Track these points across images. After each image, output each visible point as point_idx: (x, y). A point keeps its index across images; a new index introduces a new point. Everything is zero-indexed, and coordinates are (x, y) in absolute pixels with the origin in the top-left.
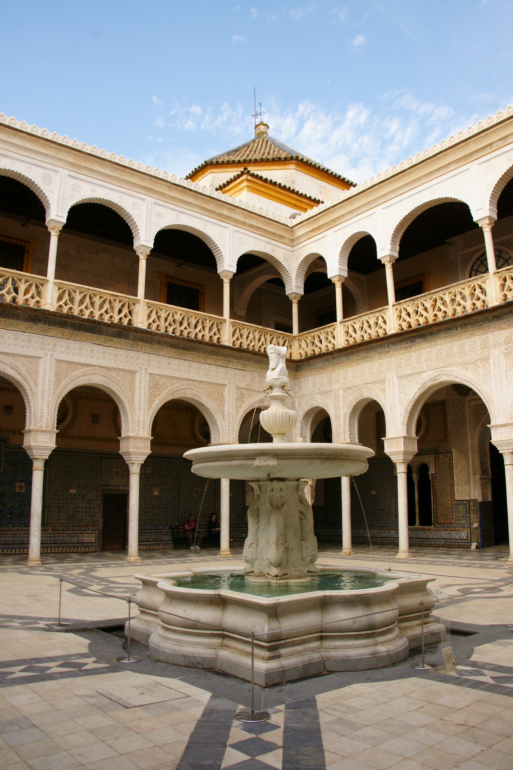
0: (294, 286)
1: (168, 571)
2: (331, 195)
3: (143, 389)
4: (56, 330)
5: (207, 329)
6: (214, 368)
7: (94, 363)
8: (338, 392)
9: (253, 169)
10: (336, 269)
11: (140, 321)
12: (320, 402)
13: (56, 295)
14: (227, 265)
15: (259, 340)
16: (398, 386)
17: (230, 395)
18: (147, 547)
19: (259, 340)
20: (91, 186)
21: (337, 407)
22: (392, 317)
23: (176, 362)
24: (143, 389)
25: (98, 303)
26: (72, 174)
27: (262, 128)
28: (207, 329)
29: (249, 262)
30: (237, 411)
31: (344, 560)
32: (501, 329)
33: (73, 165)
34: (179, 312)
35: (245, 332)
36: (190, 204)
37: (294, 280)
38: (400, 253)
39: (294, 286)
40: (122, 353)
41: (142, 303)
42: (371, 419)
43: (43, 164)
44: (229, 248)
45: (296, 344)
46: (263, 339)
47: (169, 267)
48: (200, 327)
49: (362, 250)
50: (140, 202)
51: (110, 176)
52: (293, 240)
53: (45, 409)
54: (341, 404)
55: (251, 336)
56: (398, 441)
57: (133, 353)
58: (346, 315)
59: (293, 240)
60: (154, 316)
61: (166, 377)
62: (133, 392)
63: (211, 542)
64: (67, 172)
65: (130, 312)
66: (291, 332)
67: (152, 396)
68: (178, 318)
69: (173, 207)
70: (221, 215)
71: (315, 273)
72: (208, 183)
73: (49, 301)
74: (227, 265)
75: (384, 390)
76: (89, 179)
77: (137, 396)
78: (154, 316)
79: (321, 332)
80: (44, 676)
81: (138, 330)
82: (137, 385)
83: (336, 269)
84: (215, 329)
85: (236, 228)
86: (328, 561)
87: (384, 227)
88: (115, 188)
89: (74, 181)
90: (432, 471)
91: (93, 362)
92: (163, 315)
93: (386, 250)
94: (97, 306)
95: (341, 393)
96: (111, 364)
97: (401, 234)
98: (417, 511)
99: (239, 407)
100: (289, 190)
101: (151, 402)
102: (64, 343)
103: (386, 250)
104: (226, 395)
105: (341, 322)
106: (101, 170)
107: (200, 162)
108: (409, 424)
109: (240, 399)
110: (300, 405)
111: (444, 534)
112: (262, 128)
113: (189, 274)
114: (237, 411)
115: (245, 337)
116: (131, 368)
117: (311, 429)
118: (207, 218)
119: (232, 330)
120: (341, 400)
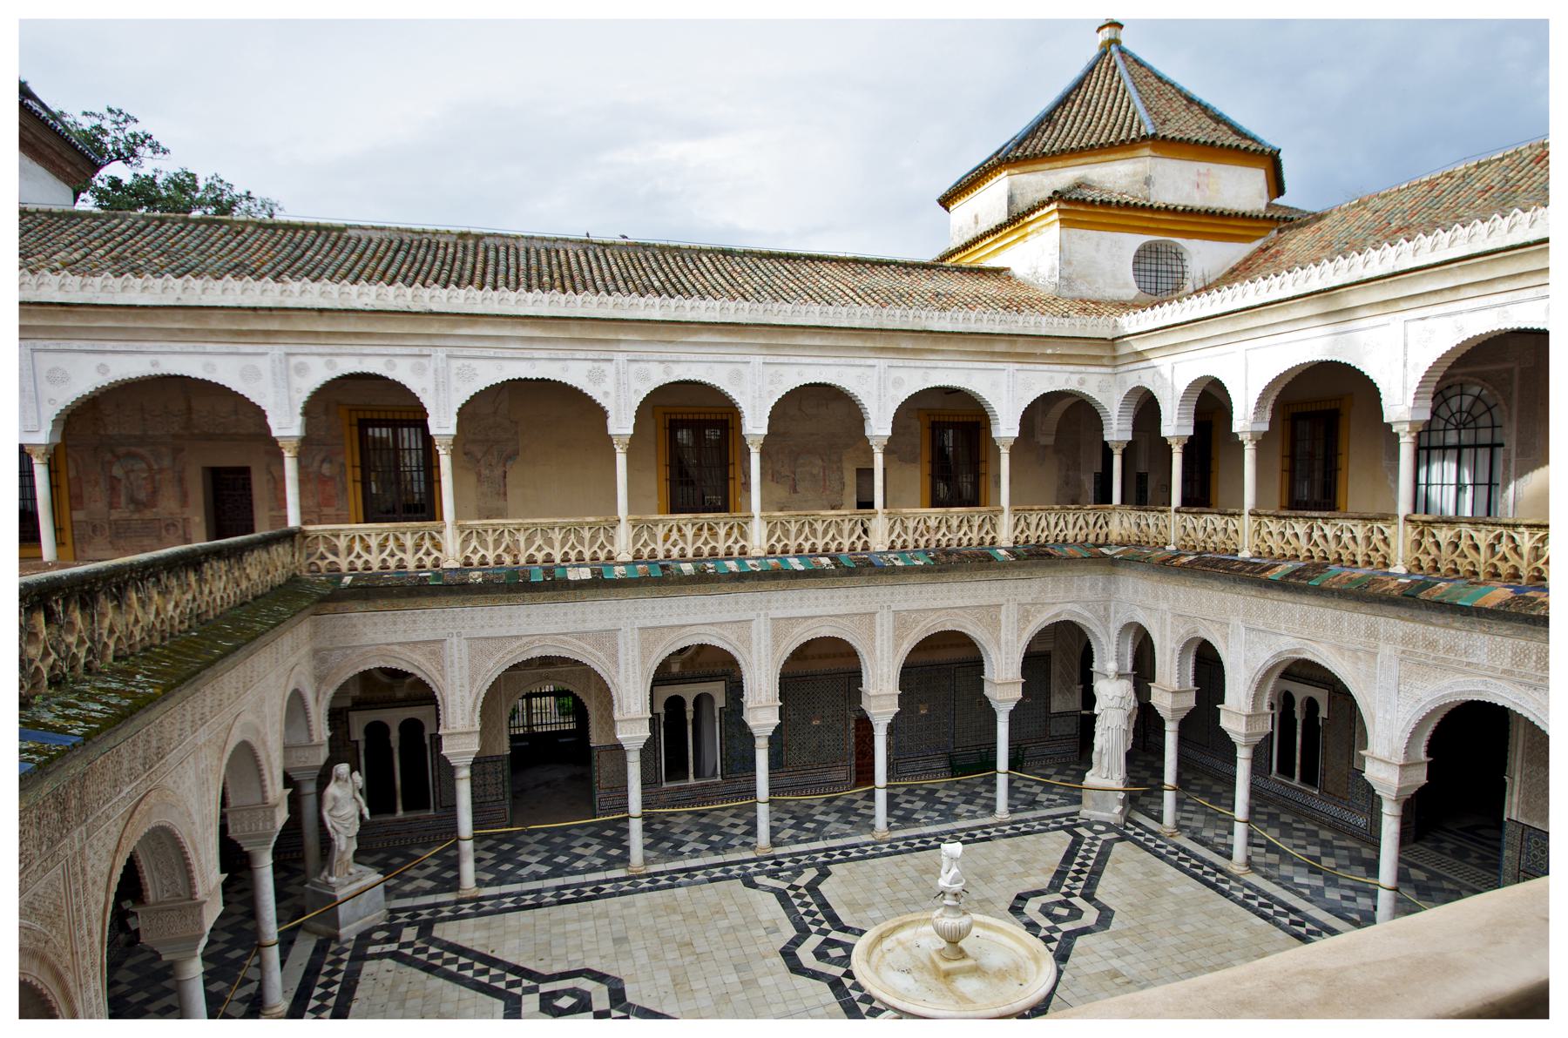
4: (766, 585)
5: (975, 529)
6: (984, 585)
7: (820, 612)
13: (765, 533)
15: (1056, 524)
17: (1008, 616)
19: (1056, 524)
20: (796, 369)
21: (1163, 636)
23: (930, 588)
26: (769, 359)
28: (975, 529)
30: (1019, 636)
32: (1399, 617)
33: (768, 346)
35: (1033, 520)
36: (943, 351)
37: (1115, 422)
38: (1271, 423)
40: (855, 592)
41: (880, 516)
43: (728, 358)
45: (1115, 520)
46: (1062, 523)
48: (965, 528)
50: (868, 371)
51: (820, 347)
52: (1115, 358)
53: (764, 679)
54: (1168, 633)
55: (1043, 523)
57: (870, 590)
59: (1115, 358)
60: (898, 528)
61: (917, 611)
62: (873, 640)
64: (760, 359)
65: (865, 531)
66: (1110, 502)
67: (898, 638)
68: (933, 523)
69: (918, 363)
70: (993, 353)
73: (756, 543)
75: (1225, 637)
76: (793, 360)
77: (878, 643)
78: (898, 528)
82: (878, 629)
84: (987, 526)
85: (1018, 366)
87: (1250, 372)
88: (831, 361)
89: (772, 369)
90: (1323, 713)
91: (818, 612)
92: (911, 524)
93: (1245, 418)
94: (820, 534)
95: (1169, 617)
96: (843, 610)
97: (1276, 393)
98: (1298, 761)
99: (1021, 630)
101: (897, 647)
102: (780, 595)
104: (1003, 617)
105: (1177, 511)
106: (808, 342)
109: (1025, 617)
110: (1116, 612)
111: (1334, 810)
114: (1019, 636)
115: (1033, 527)
116: (869, 610)
117: (1134, 639)
118: (970, 365)
119: (1013, 522)
120: (1169, 628)
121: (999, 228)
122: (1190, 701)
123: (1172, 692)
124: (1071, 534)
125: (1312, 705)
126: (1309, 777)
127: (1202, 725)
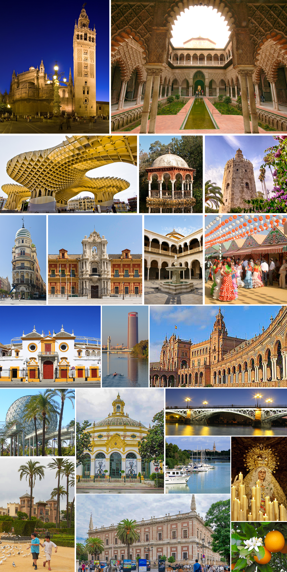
0: (178, 248)
1: (163, 281)
2: (182, 238)
3: (160, 260)
8: (183, 261)
10: (183, 246)
11: (160, 252)
14: (170, 246)
16: (190, 260)
18: (161, 279)
22: (189, 252)
24: (160, 260)
25: (155, 250)
29: (173, 246)
39: (178, 248)
42: (187, 264)
44: (170, 244)
47: (163, 246)
49: (185, 244)
56: (190, 266)
63: (168, 278)
71: (180, 247)
72: (168, 236)
74: (170, 246)
80: (149, 294)
83: (183, 246)
86: (182, 280)
87: (188, 242)
93: (188, 244)
103: (188, 244)
113: (166, 247)
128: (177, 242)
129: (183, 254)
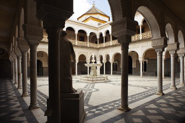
0: (98, 37)
8: (104, 53)
9: (93, 16)
10: (104, 35)
12: (101, 54)
14: (88, 35)
17: (89, 53)
18: (78, 74)
27: (94, 5)
29: (91, 33)
31: (104, 75)
34: (82, 42)
39: (98, 37)
42: (108, 57)
44: (88, 32)
45: (98, 46)
47: (80, 34)
49: (107, 32)
56: (111, 60)
58: (105, 42)
74: (88, 35)
79: (102, 44)
81: (76, 45)
83: (104, 35)
90: (117, 64)
100: (98, 19)
101: (78, 55)
107: (83, 14)
108: (113, 58)
109: (90, 54)
111: (118, 72)
112: (94, 5)
113: (82, 34)
121: (85, 20)
122: (106, 61)
123: (104, 61)
124: (94, 46)
125: (116, 63)
126: (116, 71)
127: (108, 63)
128: (96, 29)
129: (104, 44)
